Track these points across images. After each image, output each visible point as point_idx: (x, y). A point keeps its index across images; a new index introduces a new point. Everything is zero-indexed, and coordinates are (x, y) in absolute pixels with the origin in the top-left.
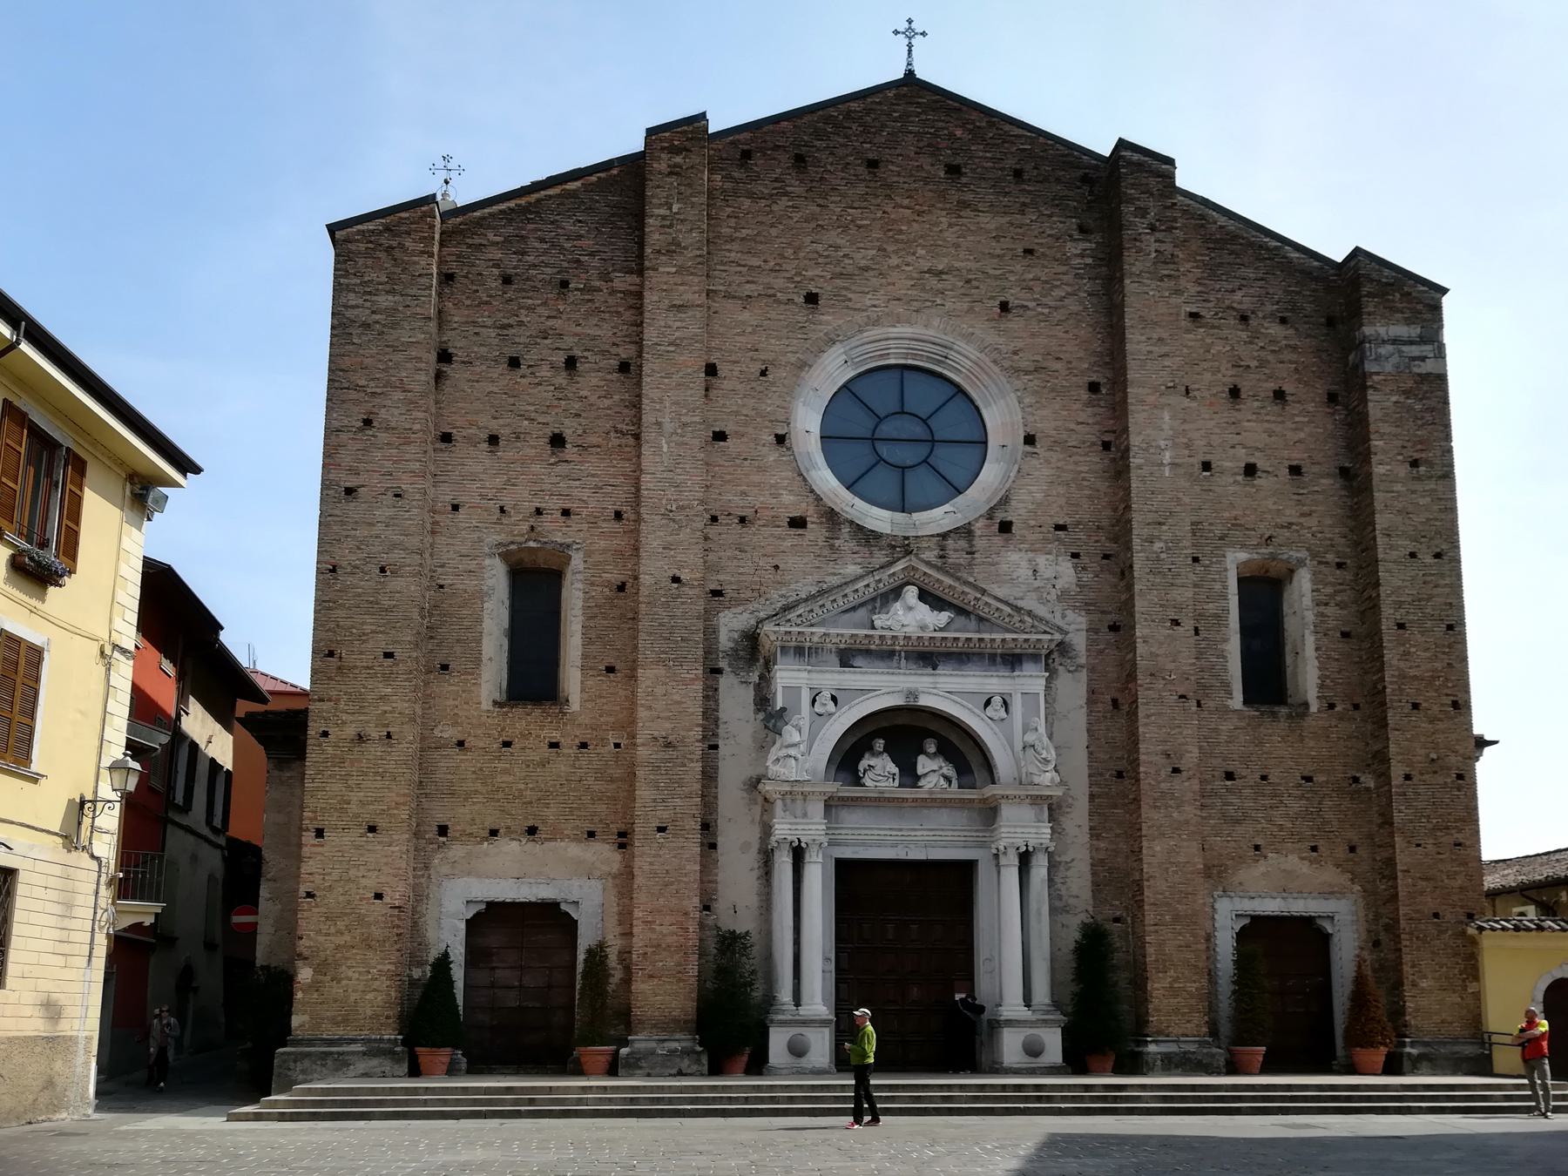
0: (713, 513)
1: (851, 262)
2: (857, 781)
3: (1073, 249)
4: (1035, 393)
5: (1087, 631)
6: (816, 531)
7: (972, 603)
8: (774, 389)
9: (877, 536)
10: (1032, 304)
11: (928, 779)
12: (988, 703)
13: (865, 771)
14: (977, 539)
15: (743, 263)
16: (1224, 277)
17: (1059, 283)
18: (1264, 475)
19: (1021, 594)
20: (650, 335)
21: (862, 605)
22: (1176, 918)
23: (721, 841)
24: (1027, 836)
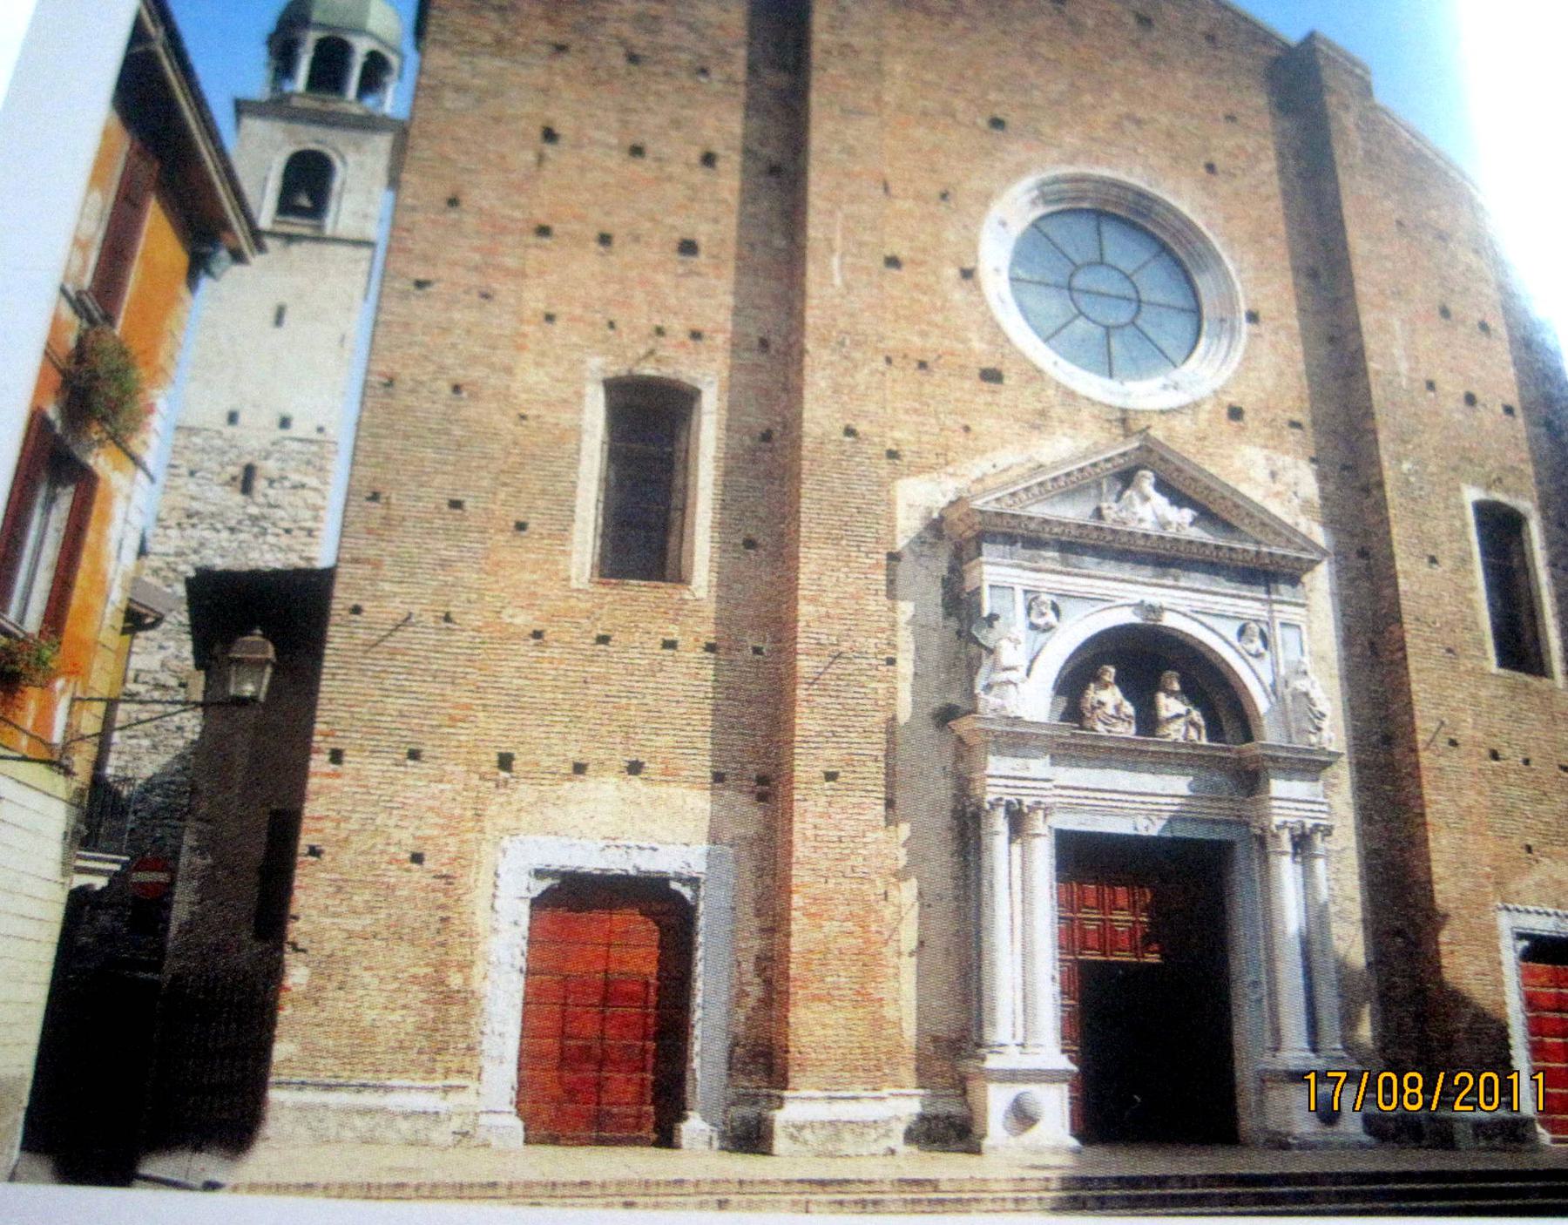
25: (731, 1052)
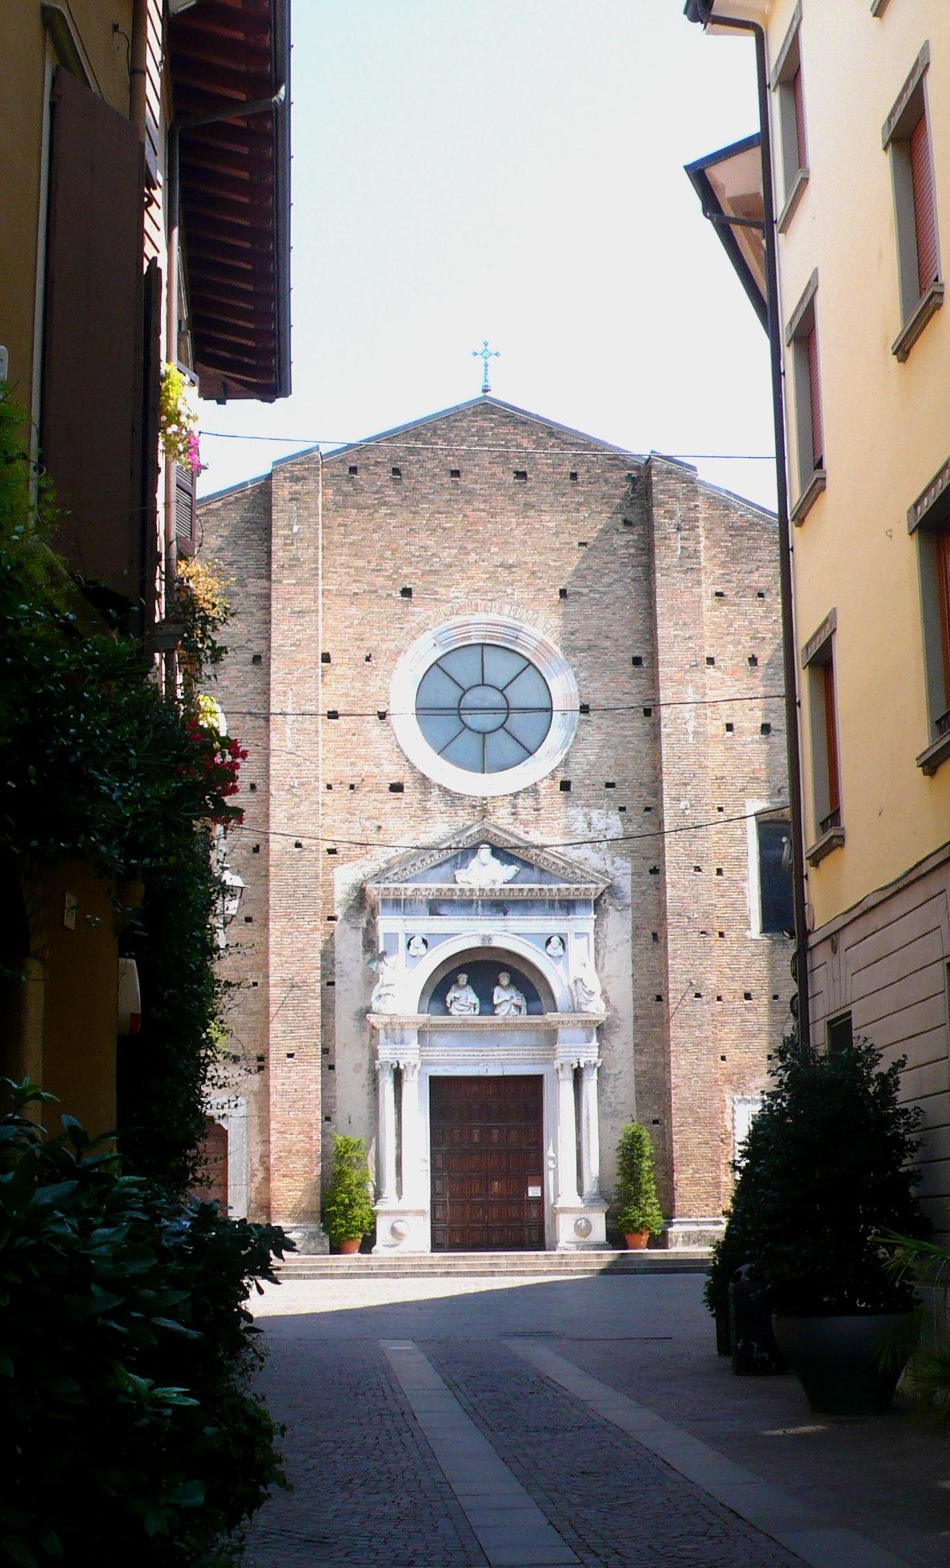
1: (438, 560)
2: (446, 1012)
3: (619, 540)
4: (589, 668)
5: (632, 874)
6: (411, 794)
8: (377, 673)
10: (585, 591)
11: (503, 1007)
12: (548, 942)
13: (451, 1002)
14: (542, 797)
15: (351, 564)
16: (744, 560)
17: (607, 571)
18: (778, 733)
20: (276, 640)
21: (446, 861)
22: (697, 1121)
23: (338, 1063)
25: (249, 1207)
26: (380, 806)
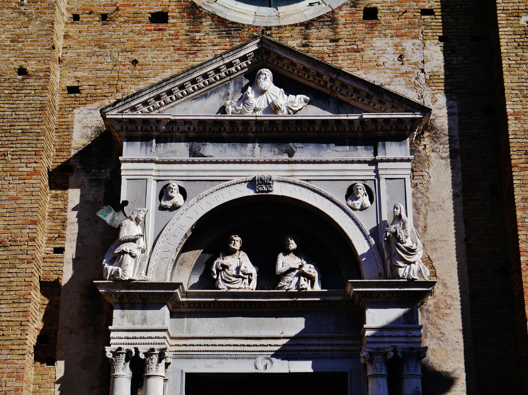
0: (75, 12)
5: (459, 115)
7: (329, 85)
9: (238, 27)
11: (289, 278)
13: (218, 271)
14: (340, 26)
19: (388, 80)
24: (394, 340)
26: (136, 38)
